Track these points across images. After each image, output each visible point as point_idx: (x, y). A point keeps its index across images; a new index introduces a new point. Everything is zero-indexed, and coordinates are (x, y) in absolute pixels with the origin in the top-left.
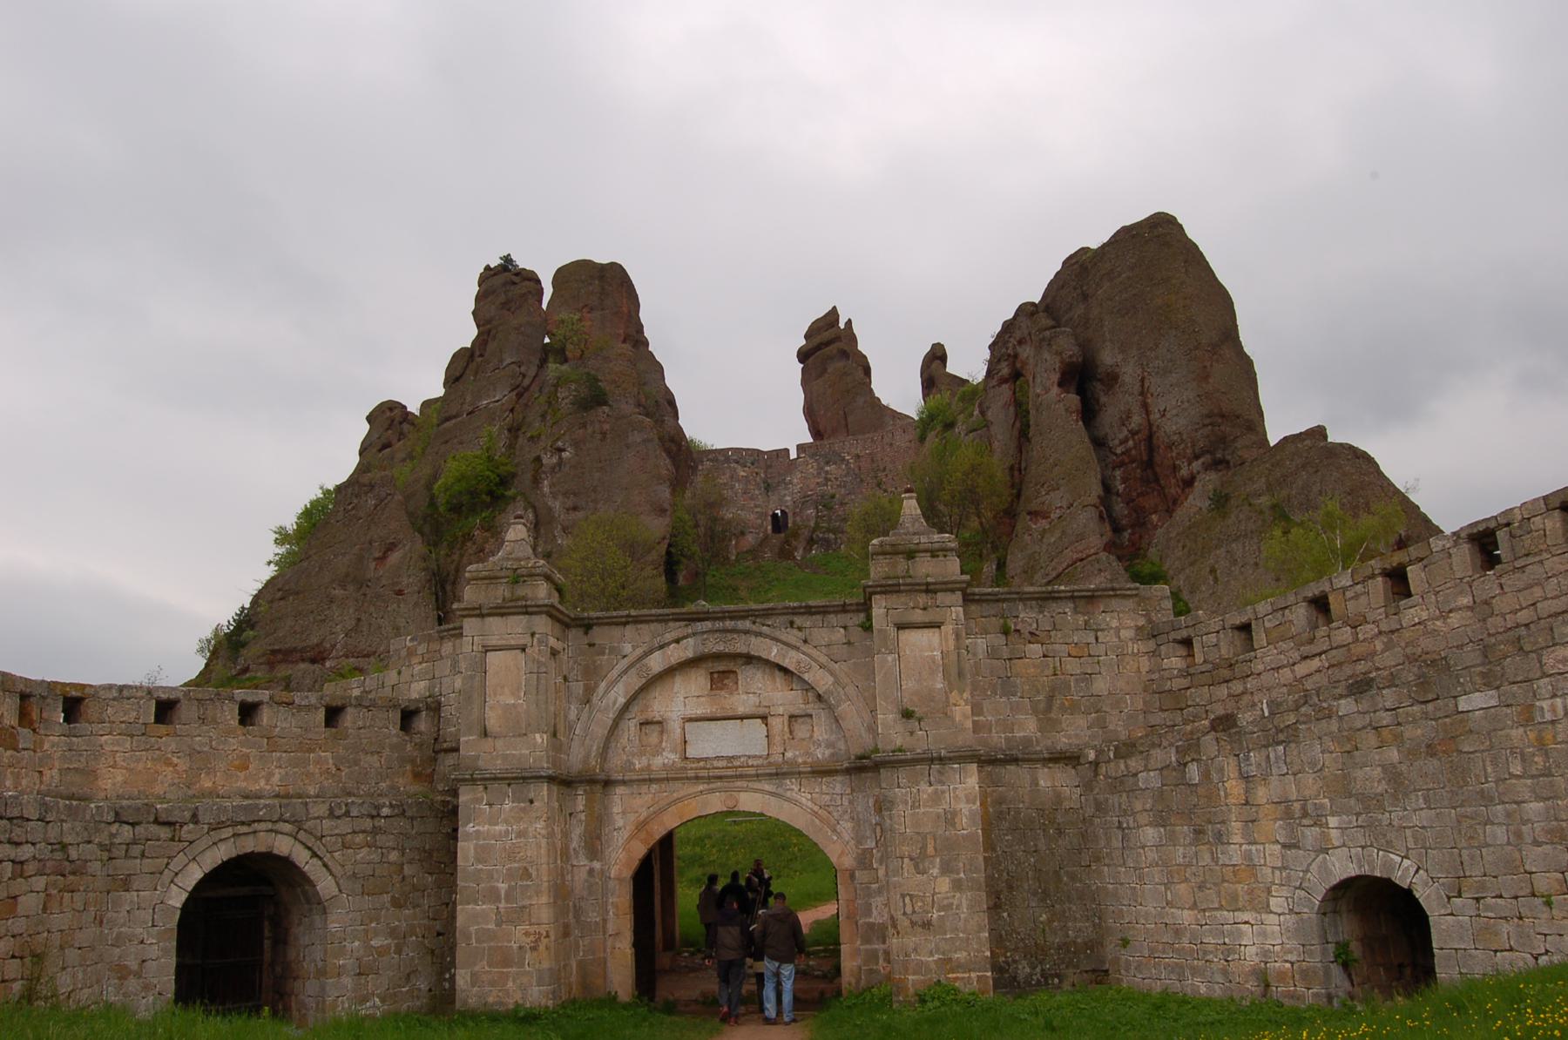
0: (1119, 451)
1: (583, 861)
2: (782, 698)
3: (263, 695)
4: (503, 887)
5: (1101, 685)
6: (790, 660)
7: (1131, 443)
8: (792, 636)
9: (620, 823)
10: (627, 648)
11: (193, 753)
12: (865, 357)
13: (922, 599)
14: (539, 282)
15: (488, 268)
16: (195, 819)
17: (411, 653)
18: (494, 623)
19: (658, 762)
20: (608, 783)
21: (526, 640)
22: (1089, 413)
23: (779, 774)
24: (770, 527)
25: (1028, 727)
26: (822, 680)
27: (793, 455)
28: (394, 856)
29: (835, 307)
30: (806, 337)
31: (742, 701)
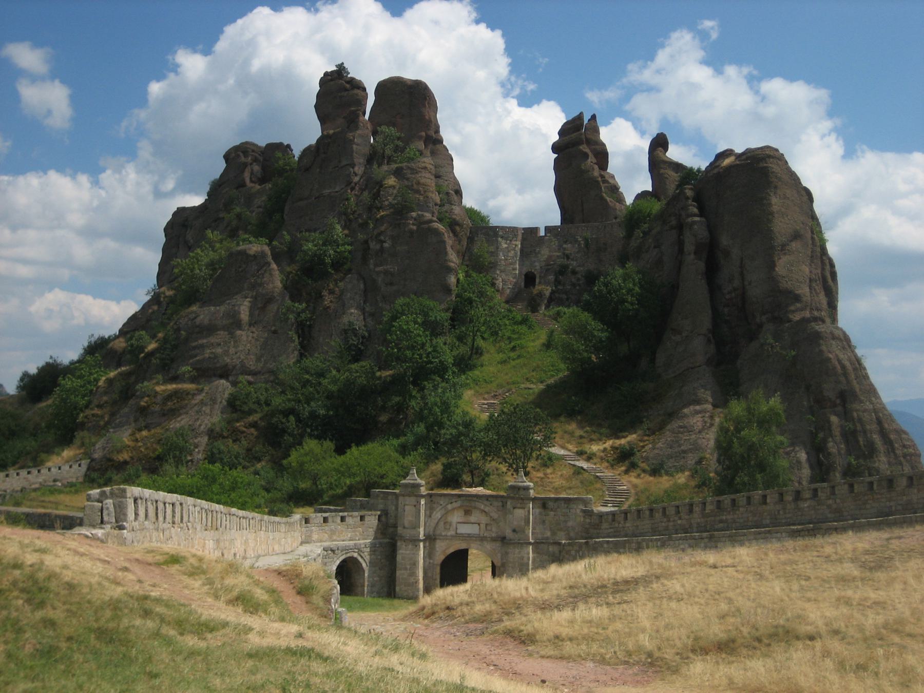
0: (728, 297)
1: (427, 560)
2: (484, 520)
3: (346, 514)
4: (408, 567)
5: (570, 524)
6: (487, 509)
7: (733, 294)
8: (488, 503)
9: (438, 549)
10: (442, 503)
11: (331, 530)
12: (604, 145)
13: (520, 501)
14: (364, 89)
15: (326, 74)
16: (338, 549)
17: (378, 496)
18: (407, 498)
19: (449, 534)
20: (435, 539)
21: (416, 503)
22: (712, 270)
23: (482, 539)
24: (523, 284)
25: (548, 534)
26: (495, 515)
27: (542, 233)
28: (379, 557)
29: (581, 114)
30: (561, 133)
31: (473, 519)
